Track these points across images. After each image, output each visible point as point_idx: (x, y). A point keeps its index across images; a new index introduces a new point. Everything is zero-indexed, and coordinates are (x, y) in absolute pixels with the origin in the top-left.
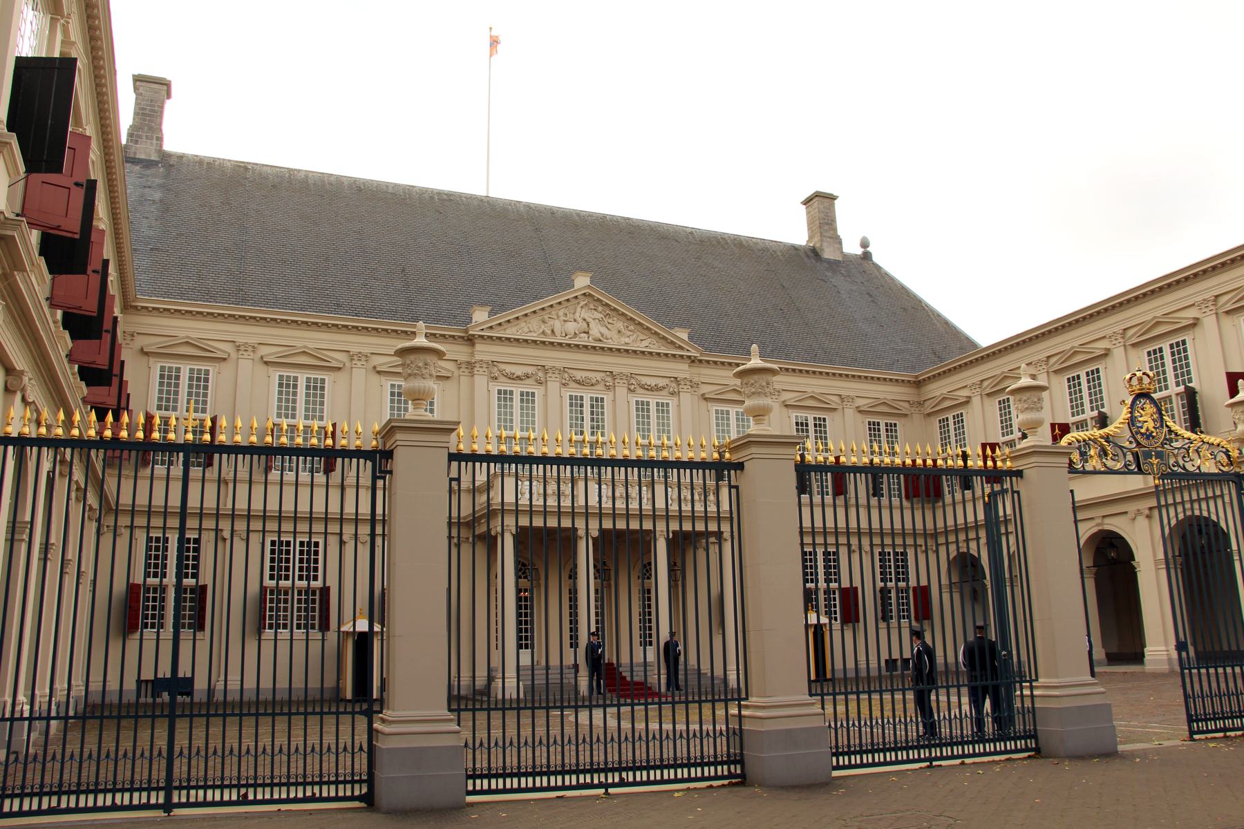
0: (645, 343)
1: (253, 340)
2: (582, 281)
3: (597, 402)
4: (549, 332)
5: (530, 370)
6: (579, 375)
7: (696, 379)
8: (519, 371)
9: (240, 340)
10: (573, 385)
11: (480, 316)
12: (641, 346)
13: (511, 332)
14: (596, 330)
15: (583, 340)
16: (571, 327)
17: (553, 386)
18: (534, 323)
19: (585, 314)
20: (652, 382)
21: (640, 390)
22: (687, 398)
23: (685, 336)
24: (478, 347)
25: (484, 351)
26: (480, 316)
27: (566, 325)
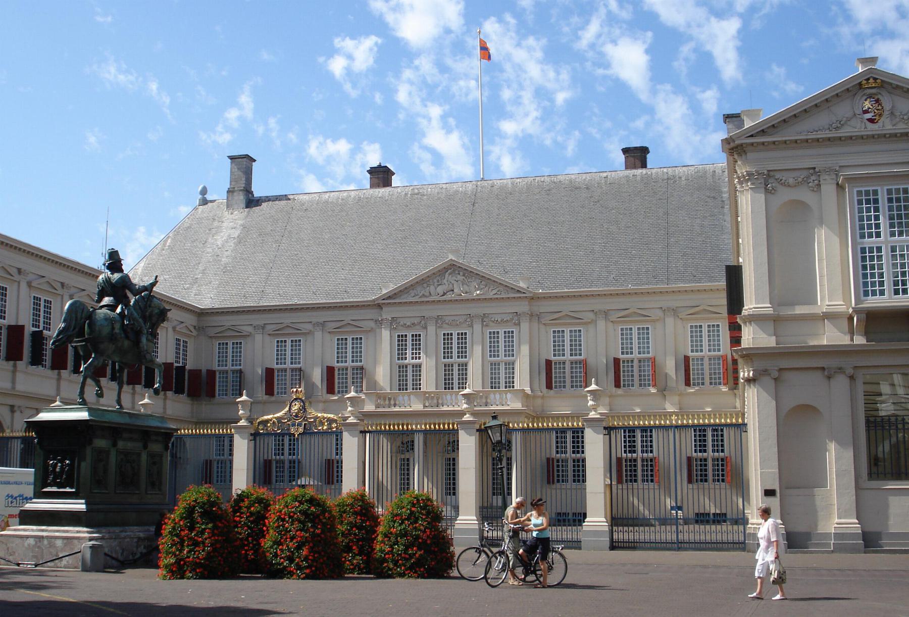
0: (494, 292)
1: (262, 323)
4: (427, 294)
5: (416, 321)
6: (447, 319)
9: (255, 323)
10: (445, 326)
12: (491, 295)
15: (448, 297)
16: (440, 290)
17: (431, 329)
19: (452, 279)
21: (491, 324)
22: (525, 326)
25: (387, 314)
27: (436, 291)
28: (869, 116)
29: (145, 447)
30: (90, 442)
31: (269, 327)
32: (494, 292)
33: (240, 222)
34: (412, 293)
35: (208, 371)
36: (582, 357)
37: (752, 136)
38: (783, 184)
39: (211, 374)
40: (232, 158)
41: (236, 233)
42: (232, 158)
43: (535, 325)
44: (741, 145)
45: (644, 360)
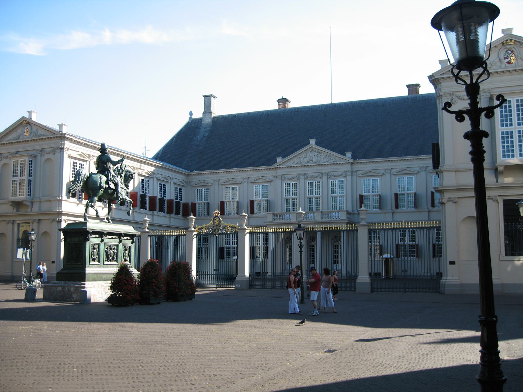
1: (218, 179)
2: (313, 142)
3: (317, 183)
5: (294, 176)
7: (355, 170)
8: (290, 176)
9: (215, 179)
11: (279, 160)
13: (288, 164)
14: (314, 160)
16: (306, 160)
17: (302, 180)
18: (296, 160)
19: (312, 154)
20: (336, 173)
21: (332, 177)
23: (349, 155)
24: (279, 171)
25: (280, 172)
26: (279, 160)
28: (508, 60)
29: (102, 241)
30: (88, 240)
31: (221, 181)
32: (333, 160)
33: (209, 128)
34: (292, 161)
35: (192, 203)
36: (379, 193)
37: (443, 74)
38: (461, 99)
39: (194, 205)
40: (203, 96)
41: (207, 134)
42: (203, 96)
43: (354, 177)
44: (438, 78)
45: (410, 194)
